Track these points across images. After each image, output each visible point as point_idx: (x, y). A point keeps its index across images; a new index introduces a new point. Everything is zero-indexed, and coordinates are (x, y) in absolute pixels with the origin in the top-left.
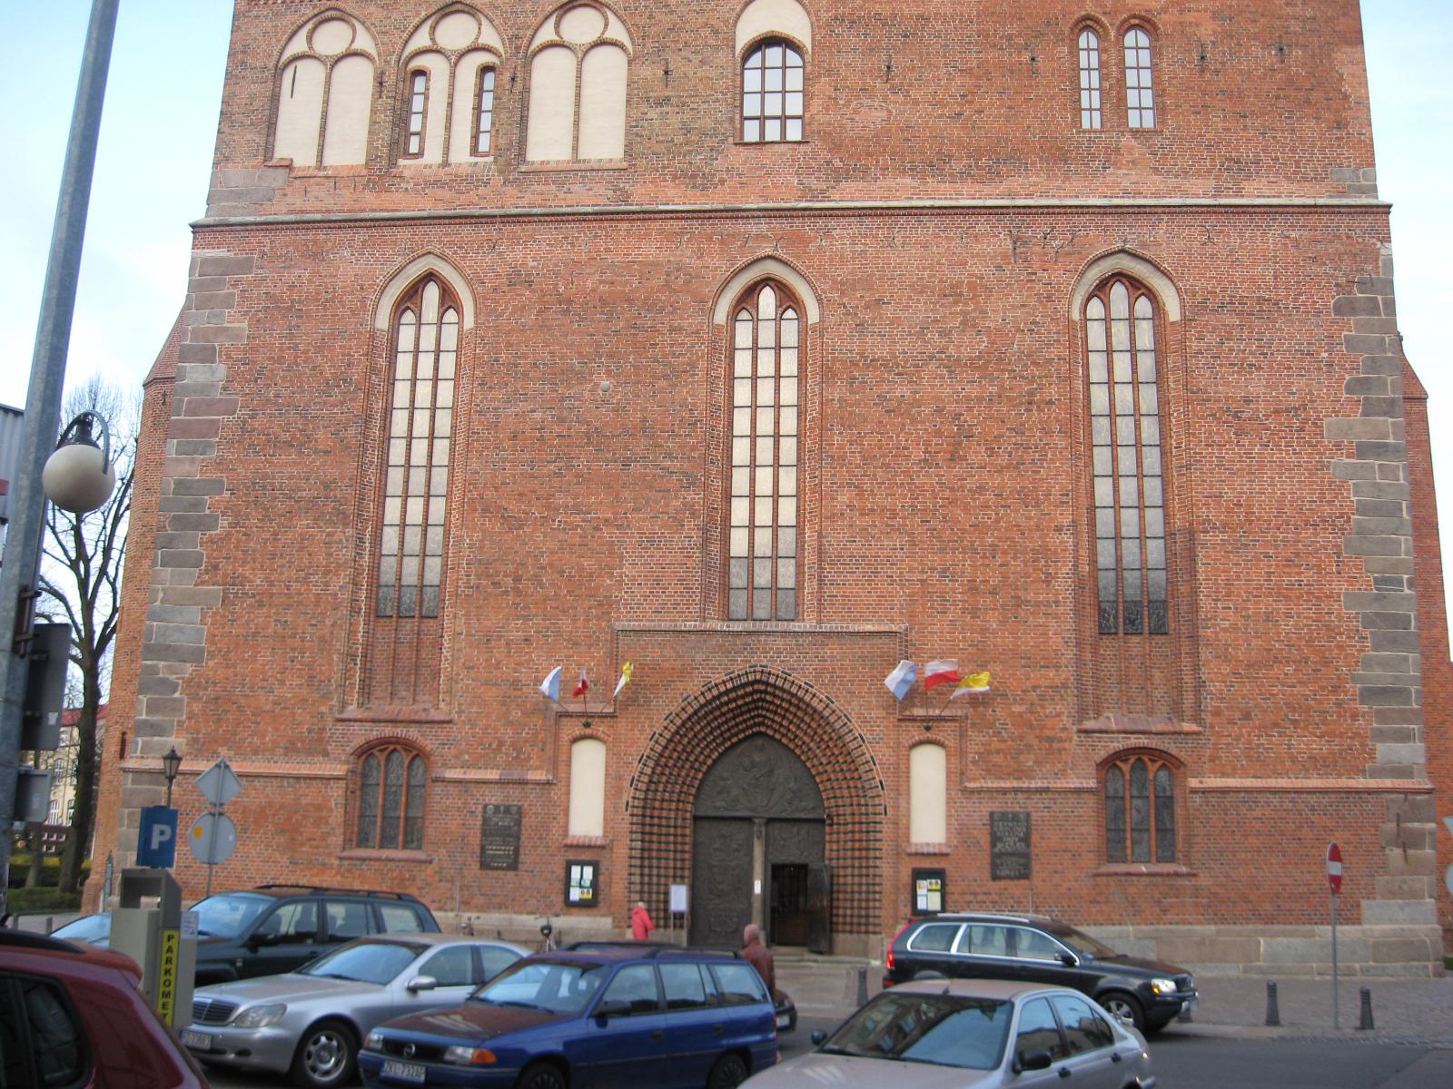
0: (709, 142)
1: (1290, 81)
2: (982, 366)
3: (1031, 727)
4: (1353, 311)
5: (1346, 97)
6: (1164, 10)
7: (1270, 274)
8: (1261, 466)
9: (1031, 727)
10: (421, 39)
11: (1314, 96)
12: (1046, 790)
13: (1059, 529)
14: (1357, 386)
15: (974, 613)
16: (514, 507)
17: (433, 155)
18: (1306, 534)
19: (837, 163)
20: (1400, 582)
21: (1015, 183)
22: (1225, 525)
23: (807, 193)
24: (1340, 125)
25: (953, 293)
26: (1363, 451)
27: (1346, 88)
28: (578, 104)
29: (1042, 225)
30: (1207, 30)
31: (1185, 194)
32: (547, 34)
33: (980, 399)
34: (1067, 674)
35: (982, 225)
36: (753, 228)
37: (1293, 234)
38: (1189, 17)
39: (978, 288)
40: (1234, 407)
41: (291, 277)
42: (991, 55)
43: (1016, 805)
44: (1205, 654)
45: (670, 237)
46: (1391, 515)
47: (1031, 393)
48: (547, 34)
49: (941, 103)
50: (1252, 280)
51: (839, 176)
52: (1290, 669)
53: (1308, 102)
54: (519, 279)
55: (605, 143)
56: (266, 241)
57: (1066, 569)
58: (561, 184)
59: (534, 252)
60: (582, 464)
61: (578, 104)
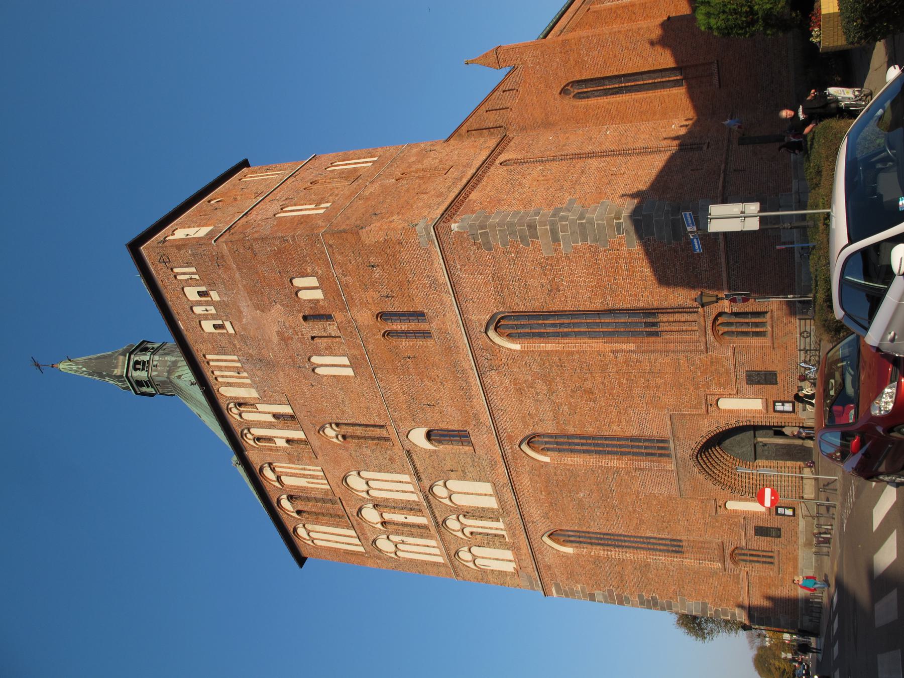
0: (476, 460)
2: (549, 383)
3: (706, 369)
4: (489, 243)
5: (385, 240)
6: (371, 310)
7: (480, 277)
8: (572, 282)
9: (706, 369)
10: (460, 534)
11: (389, 251)
12: (735, 365)
13: (616, 358)
14: (523, 239)
15: (658, 387)
16: (635, 522)
17: (504, 533)
19: (474, 422)
20: (619, 223)
21: (465, 365)
22: (603, 296)
23: (488, 431)
24: (400, 243)
25: (520, 391)
26: (556, 239)
27: (381, 239)
28: (472, 494)
29: (482, 360)
30: (376, 295)
31: (452, 305)
32: (447, 502)
33: (564, 383)
34: (681, 356)
35: (488, 380)
37: (459, 267)
38: (370, 300)
39: (515, 382)
40: (547, 292)
41: (558, 574)
46: (585, 228)
47: (558, 366)
49: (438, 389)
50: (485, 283)
51: (479, 423)
52: (669, 271)
53: (394, 255)
54: (546, 516)
55: (487, 488)
56: (547, 580)
58: (505, 502)
59: (534, 512)
60: (615, 503)
61: (472, 494)
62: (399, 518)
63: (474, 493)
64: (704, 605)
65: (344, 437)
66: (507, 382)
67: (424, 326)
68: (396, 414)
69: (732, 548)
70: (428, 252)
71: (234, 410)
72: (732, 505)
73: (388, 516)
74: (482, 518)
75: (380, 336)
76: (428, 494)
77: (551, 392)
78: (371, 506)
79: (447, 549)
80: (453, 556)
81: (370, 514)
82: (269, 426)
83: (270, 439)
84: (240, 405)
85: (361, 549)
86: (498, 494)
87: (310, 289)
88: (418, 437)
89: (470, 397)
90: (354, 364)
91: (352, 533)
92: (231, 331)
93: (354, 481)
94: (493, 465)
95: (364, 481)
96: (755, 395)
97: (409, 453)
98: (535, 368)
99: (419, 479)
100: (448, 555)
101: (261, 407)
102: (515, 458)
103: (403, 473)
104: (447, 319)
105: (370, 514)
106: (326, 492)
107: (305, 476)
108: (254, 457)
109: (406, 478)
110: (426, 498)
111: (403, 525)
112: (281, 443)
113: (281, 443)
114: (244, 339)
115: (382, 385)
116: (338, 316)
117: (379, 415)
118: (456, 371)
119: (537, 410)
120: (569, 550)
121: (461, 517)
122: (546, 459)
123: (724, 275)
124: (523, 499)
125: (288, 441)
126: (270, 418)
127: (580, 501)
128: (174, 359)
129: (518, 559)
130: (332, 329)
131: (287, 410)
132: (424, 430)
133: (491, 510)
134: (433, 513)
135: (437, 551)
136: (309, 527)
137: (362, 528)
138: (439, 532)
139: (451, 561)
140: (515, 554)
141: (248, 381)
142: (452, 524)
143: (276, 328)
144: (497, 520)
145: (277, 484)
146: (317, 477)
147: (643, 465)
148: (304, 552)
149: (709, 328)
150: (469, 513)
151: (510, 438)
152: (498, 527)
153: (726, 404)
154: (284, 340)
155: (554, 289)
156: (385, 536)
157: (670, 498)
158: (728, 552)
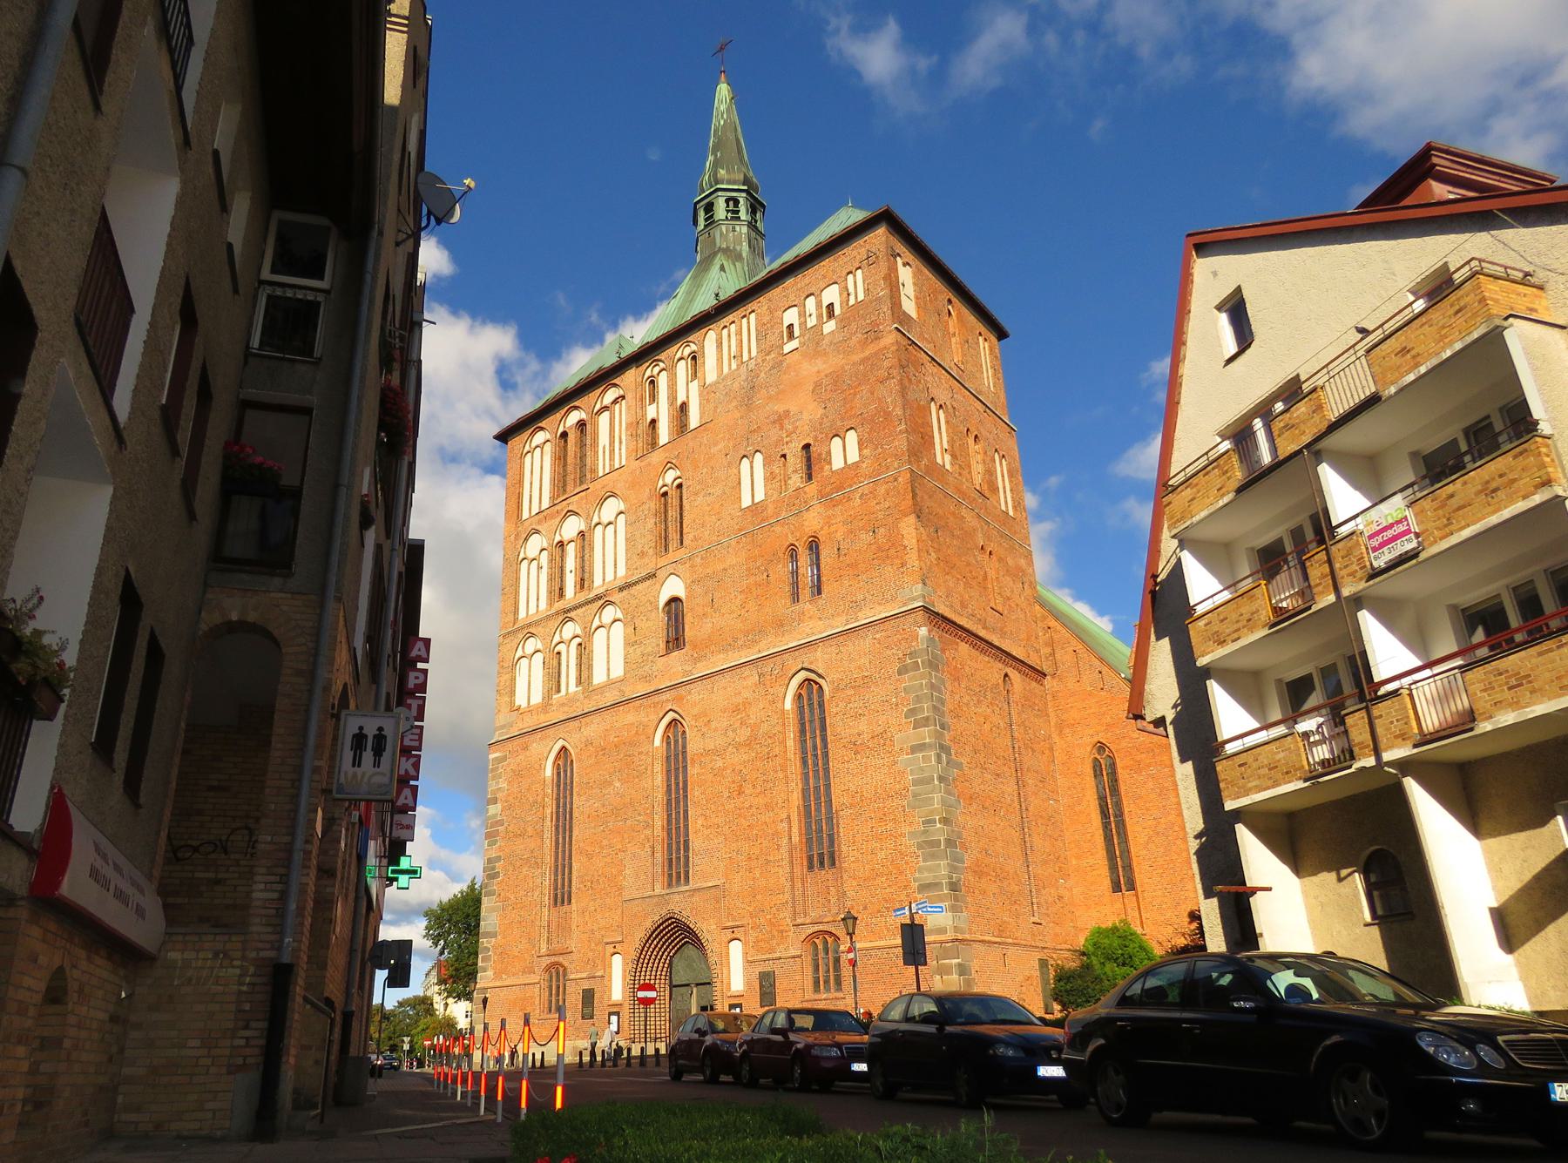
1: (880, 549)
2: (748, 744)
4: (907, 672)
10: (557, 639)
11: (892, 551)
14: (912, 712)
18: (889, 803)
21: (762, 645)
23: (686, 673)
25: (736, 710)
26: (914, 749)
27: (906, 542)
29: (769, 665)
30: (839, 536)
32: (596, 623)
34: (787, 896)
35: (746, 671)
36: (664, 697)
38: (833, 528)
39: (747, 704)
42: (751, 580)
43: (767, 968)
44: (845, 877)
45: (637, 709)
48: (596, 623)
49: (733, 612)
51: (696, 661)
54: (589, 743)
55: (618, 671)
56: (509, 745)
57: (785, 840)
59: (593, 729)
62: (571, 563)
63: (611, 655)
64: (494, 935)
65: (666, 494)
66: (746, 694)
67: (806, 593)
68: (698, 560)
69: (566, 964)
70: (894, 598)
71: (687, 351)
72: (617, 961)
73: (571, 550)
74: (579, 665)
75: (791, 540)
76: (603, 600)
77: (738, 746)
78: (583, 527)
79: (537, 623)
80: (528, 631)
81: (572, 527)
83: (653, 398)
84: (694, 358)
85: (525, 515)
86: (610, 684)
87: (844, 452)
88: (674, 587)
89: (725, 651)
90: (755, 508)
91: (546, 504)
92: (788, 348)
93: (611, 507)
94: (646, 678)
95: (612, 519)
96: (748, 983)
98: (765, 727)
99: (621, 589)
100: (530, 625)
101: (694, 386)
102: (655, 705)
103: (628, 569)
104: (815, 622)
105: (572, 527)
106: (594, 471)
107: (612, 443)
108: (631, 376)
109: (622, 571)
110: (598, 598)
111: (562, 569)
113: (651, 412)
114: (778, 365)
115: (733, 542)
116: (812, 489)
117: (695, 539)
118: (754, 633)
119: (716, 730)
120: (549, 771)
121: (578, 640)
122: (657, 742)
123: (882, 943)
124: (607, 715)
126: (681, 398)
127: (610, 783)
129: (530, 710)
130: (796, 480)
131: (694, 420)
132: (681, 594)
133: (590, 677)
134: (581, 606)
135: (532, 610)
136: (548, 447)
137: (552, 517)
138: (557, 613)
139: (522, 628)
140: (537, 707)
141: (726, 370)
142: (570, 629)
143: (793, 409)
144: (579, 682)
145: (598, 407)
146: (612, 459)
147: (658, 855)
148: (515, 442)
149: (821, 927)
150: (584, 650)
151: (680, 699)
152: (570, 684)
153: (736, 949)
154: (780, 420)
155: (856, 747)
156: (545, 545)
157: (621, 889)
158: (560, 959)
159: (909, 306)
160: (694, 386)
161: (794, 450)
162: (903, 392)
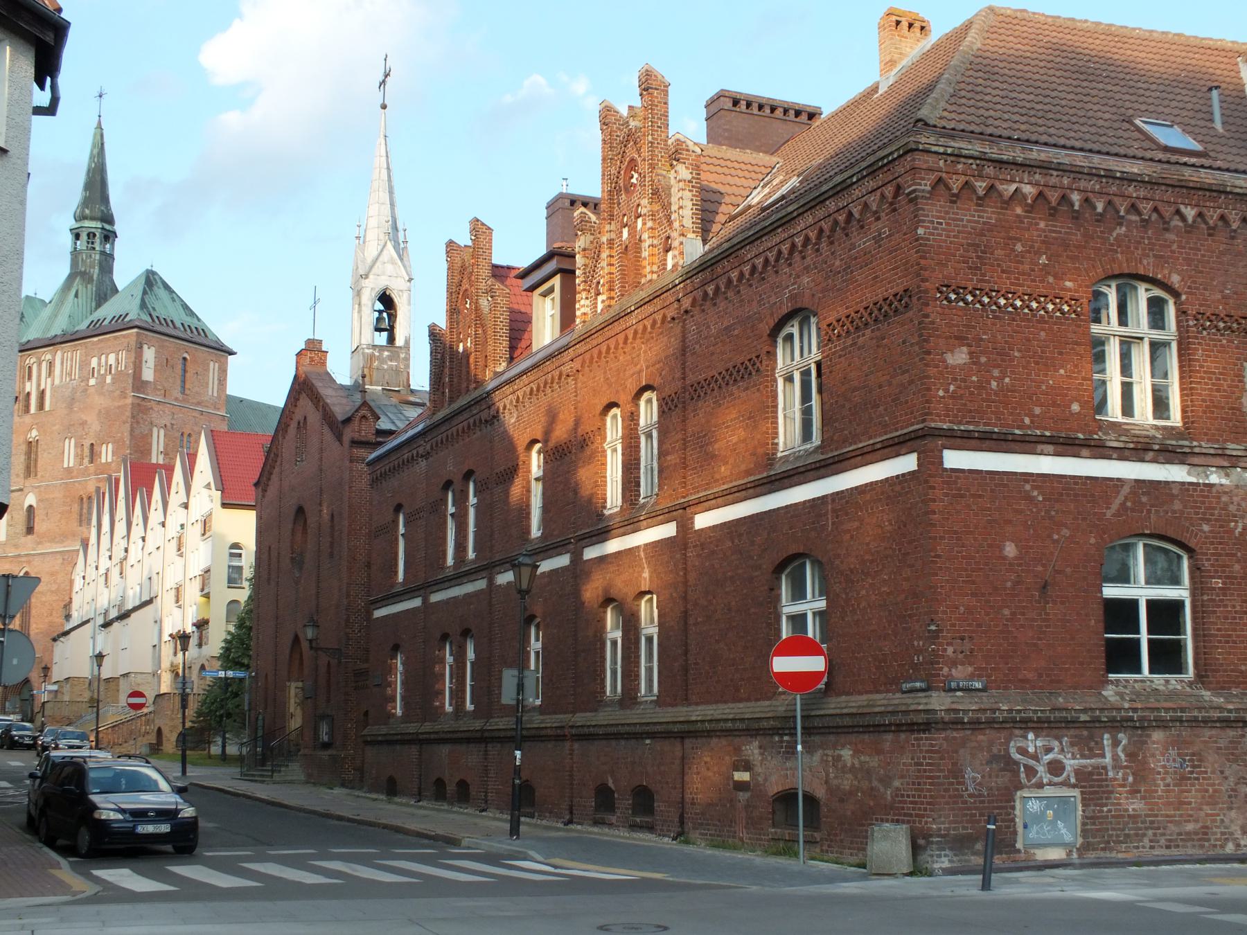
25: (52, 574)
35: (58, 556)
82: (39, 385)
83: (30, 378)
87: (107, 454)
94: (16, 546)
97: (21, 490)
112: (28, 389)
125: (29, 394)
126: (42, 387)
128: (95, 277)
130: (86, 460)
132: (35, 505)
159: (148, 374)
160: (49, 380)
161: (87, 444)
162: (132, 430)
